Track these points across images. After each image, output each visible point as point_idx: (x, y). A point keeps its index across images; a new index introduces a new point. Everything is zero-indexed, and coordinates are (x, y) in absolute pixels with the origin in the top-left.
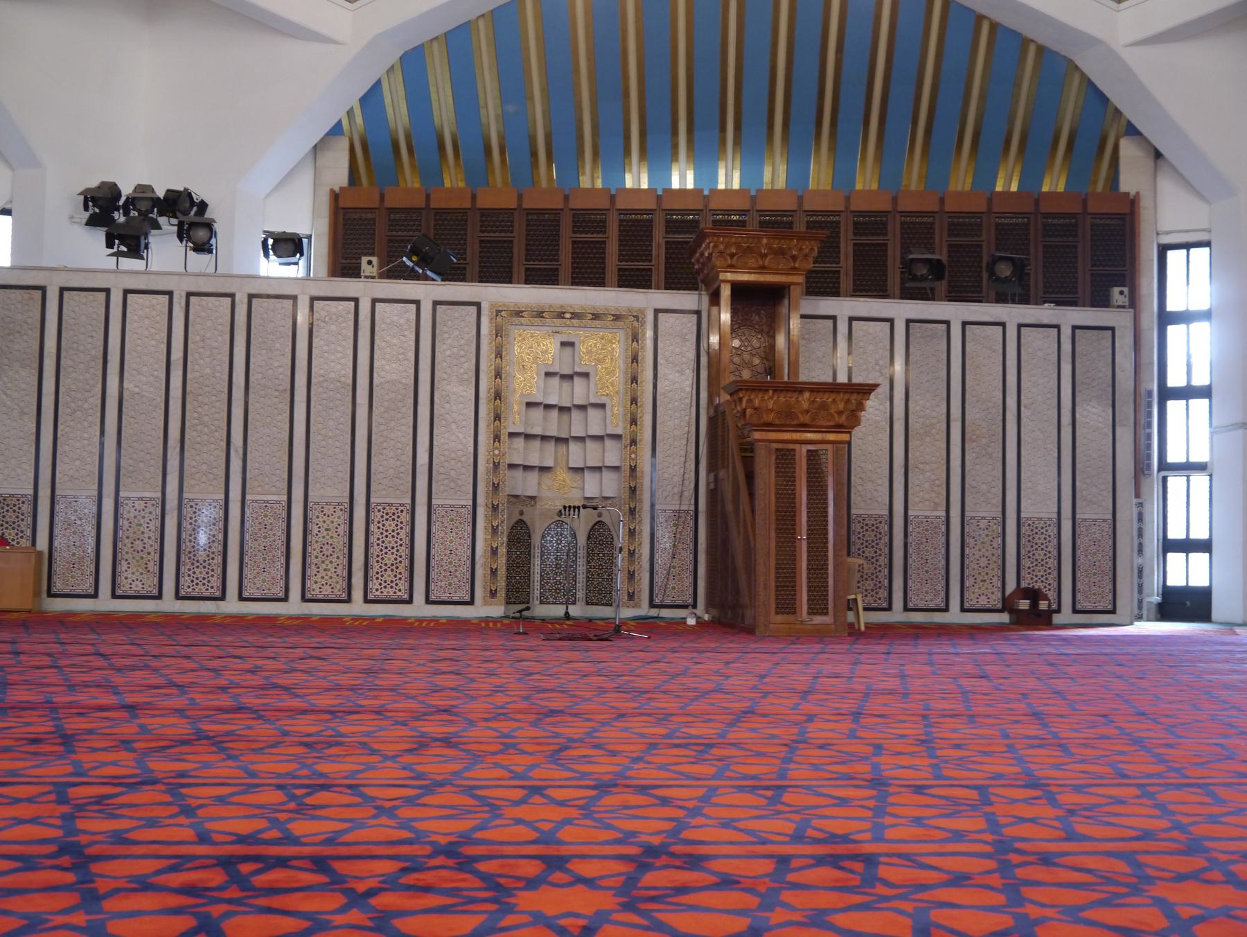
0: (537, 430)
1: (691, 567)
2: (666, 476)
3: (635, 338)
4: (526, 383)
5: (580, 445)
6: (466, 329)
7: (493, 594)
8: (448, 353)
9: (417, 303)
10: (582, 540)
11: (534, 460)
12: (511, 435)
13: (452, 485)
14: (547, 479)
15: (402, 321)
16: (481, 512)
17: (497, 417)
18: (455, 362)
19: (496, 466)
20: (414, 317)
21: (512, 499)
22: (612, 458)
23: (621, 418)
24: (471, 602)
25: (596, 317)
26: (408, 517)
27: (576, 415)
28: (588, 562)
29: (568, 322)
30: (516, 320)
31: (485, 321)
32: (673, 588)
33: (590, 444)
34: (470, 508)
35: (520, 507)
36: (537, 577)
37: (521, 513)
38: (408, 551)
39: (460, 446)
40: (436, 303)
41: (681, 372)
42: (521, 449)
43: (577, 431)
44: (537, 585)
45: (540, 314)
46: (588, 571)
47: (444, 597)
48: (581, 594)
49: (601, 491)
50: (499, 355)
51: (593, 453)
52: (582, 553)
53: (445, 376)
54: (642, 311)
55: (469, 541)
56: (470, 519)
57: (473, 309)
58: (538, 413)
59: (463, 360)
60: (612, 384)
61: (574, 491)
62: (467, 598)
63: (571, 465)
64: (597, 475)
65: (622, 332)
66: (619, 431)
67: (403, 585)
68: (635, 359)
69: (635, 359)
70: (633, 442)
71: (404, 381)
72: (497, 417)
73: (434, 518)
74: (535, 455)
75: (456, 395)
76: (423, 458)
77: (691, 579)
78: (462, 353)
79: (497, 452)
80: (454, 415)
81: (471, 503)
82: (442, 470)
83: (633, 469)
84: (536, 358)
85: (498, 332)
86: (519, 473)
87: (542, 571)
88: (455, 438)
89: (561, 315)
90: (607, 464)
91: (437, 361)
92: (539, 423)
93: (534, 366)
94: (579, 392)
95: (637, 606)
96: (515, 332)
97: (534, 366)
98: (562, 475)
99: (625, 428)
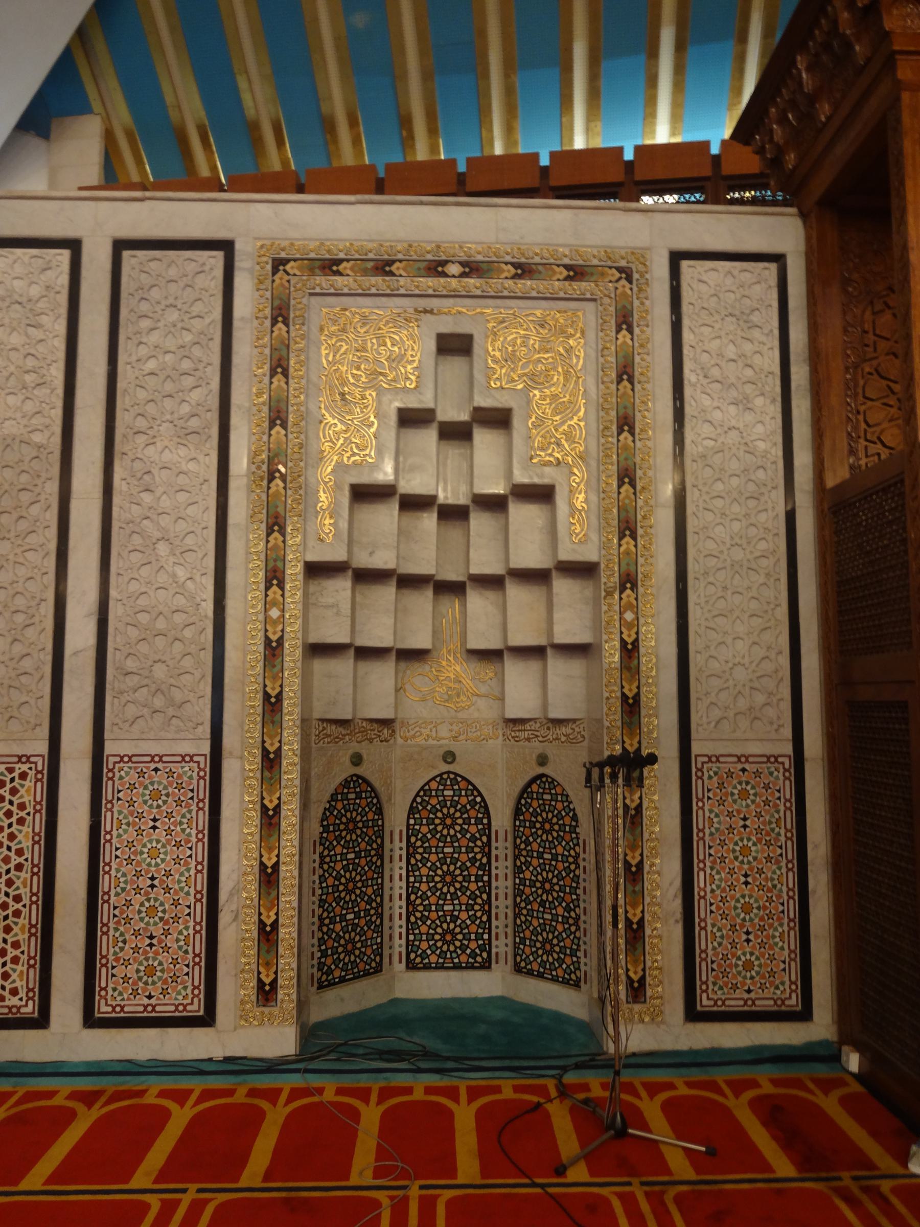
0: (383, 560)
1: (793, 909)
2: (714, 665)
3: (625, 321)
4: (351, 439)
5: (492, 595)
6: (198, 308)
7: (266, 993)
8: (151, 365)
9: (74, 246)
10: (501, 818)
11: (378, 633)
12: (316, 571)
13: (158, 702)
14: (418, 677)
15: (35, 291)
16: (231, 769)
17: (276, 524)
18: (169, 387)
19: (273, 650)
20: (64, 280)
21: (332, 729)
22: (571, 626)
23: (594, 521)
24: (207, 1019)
25: (524, 270)
26: (41, 791)
27: (480, 522)
28: (518, 870)
29: (454, 283)
30: (323, 282)
31: (243, 285)
32: (748, 966)
33: (515, 592)
34: (205, 763)
35: (355, 747)
36: (398, 907)
37: (357, 760)
38: (37, 884)
39: (180, 601)
40: (120, 246)
41: (744, 404)
42: (346, 607)
43: (485, 561)
44: (399, 925)
45: (383, 267)
46: (518, 893)
47: (134, 1007)
48: (502, 946)
49: (545, 706)
50: (279, 367)
51: (521, 616)
52: (502, 848)
53: (141, 423)
54: (641, 255)
55: (201, 851)
56: (204, 792)
57: (216, 259)
58: (384, 517)
59: (188, 381)
60: (569, 436)
61: (481, 703)
62: (196, 1008)
63: (473, 644)
64: (533, 666)
65: (590, 306)
66: (590, 554)
67: (22, 977)
68: (626, 372)
69: (626, 372)
70: (629, 581)
71: (37, 438)
72: (276, 524)
73: (108, 792)
74: (382, 619)
75: (170, 471)
76: (81, 635)
77: (794, 941)
78: (186, 365)
79: (274, 613)
80: (165, 521)
81: (206, 748)
82: (131, 664)
83: (630, 651)
84: (375, 374)
85: (281, 313)
86: (343, 666)
87: (411, 890)
88: (165, 582)
89: (436, 268)
90: (560, 639)
91: (121, 385)
92: (384, 538)
93: (371, 394)
94: (488, 466)
95: (657, 1017)
96: (320, 311)
97: (371, 394)
98: (454, 668)
99: (605, 546)
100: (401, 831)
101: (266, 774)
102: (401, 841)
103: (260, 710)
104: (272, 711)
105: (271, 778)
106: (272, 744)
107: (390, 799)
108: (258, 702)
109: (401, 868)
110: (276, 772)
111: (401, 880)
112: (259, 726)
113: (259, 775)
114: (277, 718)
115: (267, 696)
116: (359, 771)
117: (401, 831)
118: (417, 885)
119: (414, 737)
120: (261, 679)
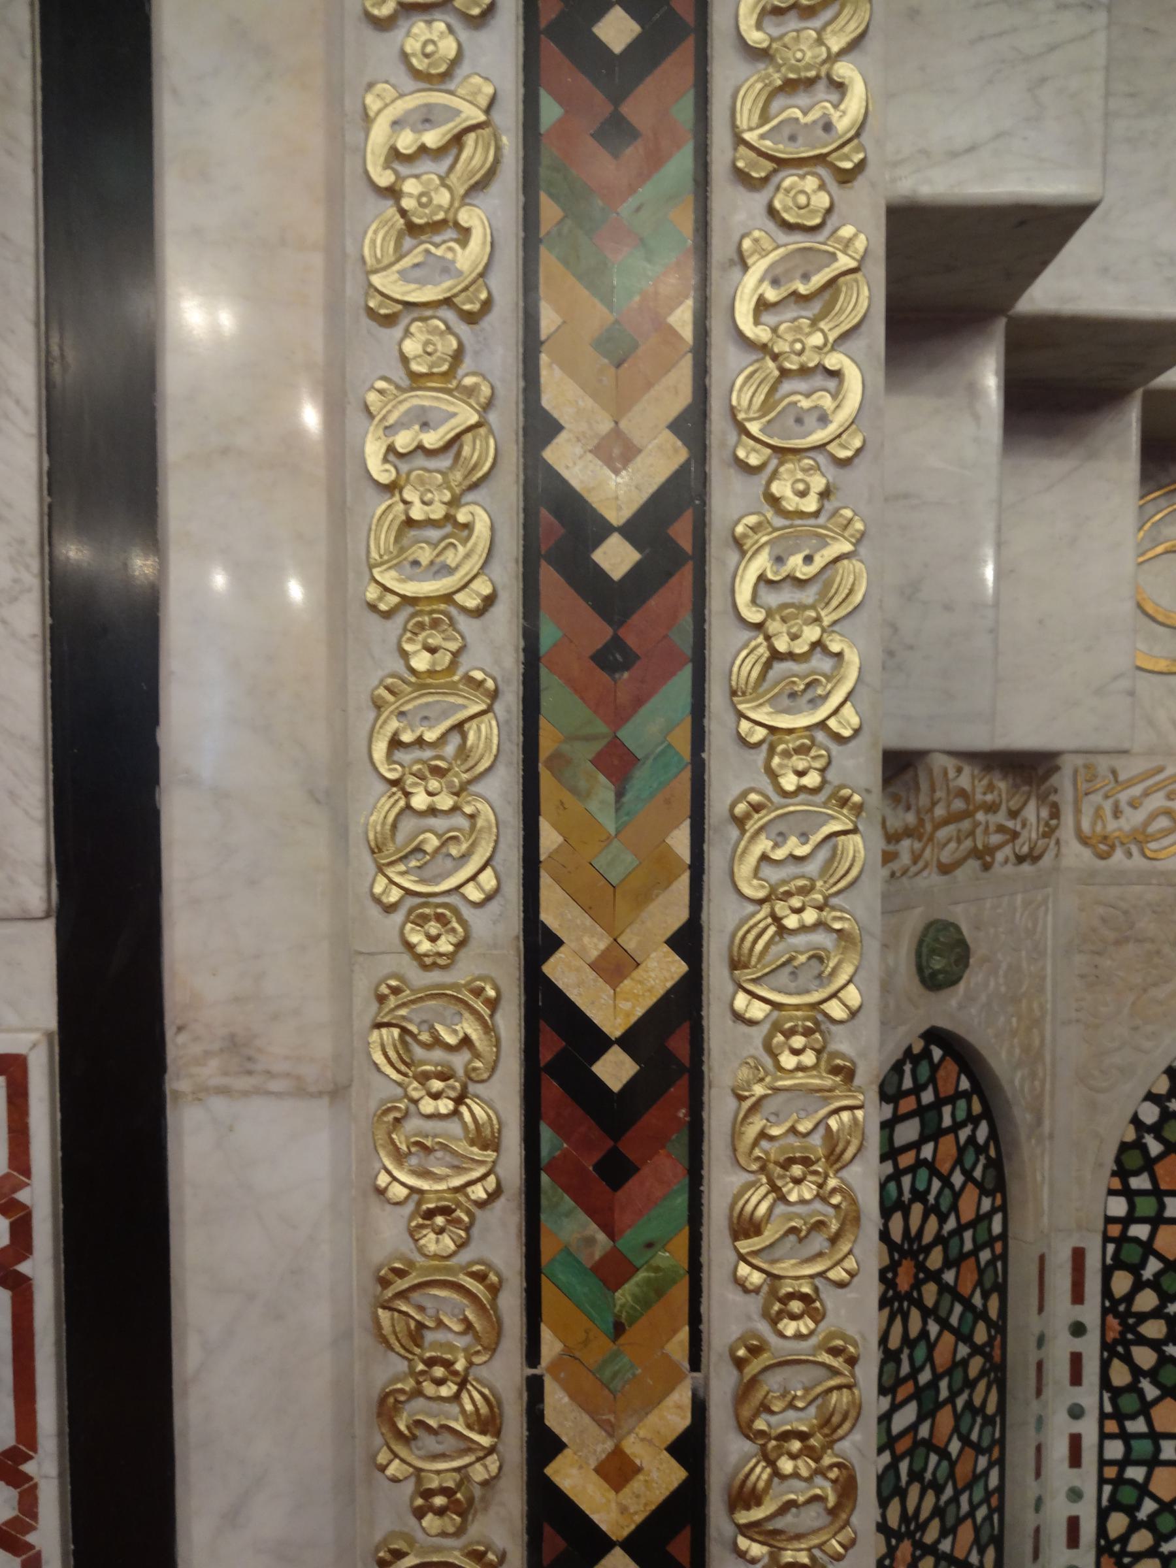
100: (1078, 1256)
101: (571, 1228)
102: (1078, 1296)
103: (494, 651)
104: (612, 658)
105: (612, 1271)
106: (615, 967)
107: (1039, 1121)
108: (482, 551)
109: (1076, 1413)
110: (655, 1218)
111: (1075, 1460)
112: (496, 799)
113: (499, 1244)
114: (657, 724)
115: (557, 528)
116: (951, 1010)
117: (1078, 1256)
118: (1136, 1473)
119: (1141, 837)
120: (496, 356)
